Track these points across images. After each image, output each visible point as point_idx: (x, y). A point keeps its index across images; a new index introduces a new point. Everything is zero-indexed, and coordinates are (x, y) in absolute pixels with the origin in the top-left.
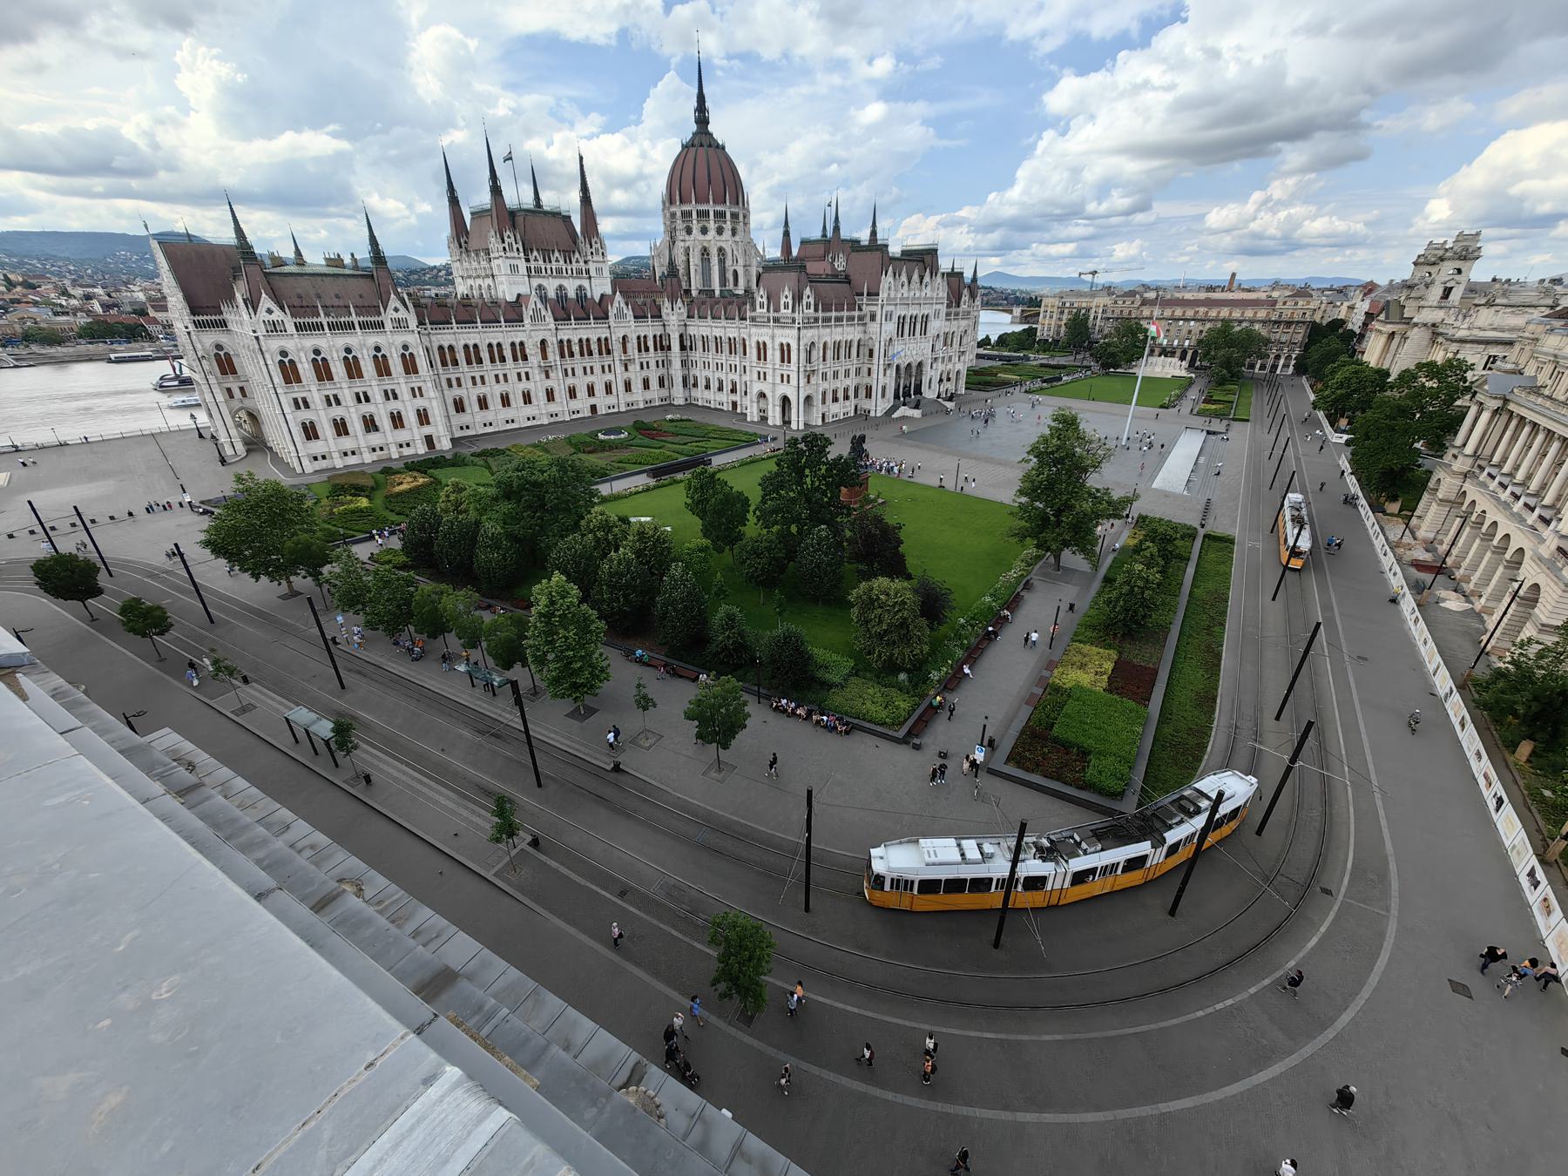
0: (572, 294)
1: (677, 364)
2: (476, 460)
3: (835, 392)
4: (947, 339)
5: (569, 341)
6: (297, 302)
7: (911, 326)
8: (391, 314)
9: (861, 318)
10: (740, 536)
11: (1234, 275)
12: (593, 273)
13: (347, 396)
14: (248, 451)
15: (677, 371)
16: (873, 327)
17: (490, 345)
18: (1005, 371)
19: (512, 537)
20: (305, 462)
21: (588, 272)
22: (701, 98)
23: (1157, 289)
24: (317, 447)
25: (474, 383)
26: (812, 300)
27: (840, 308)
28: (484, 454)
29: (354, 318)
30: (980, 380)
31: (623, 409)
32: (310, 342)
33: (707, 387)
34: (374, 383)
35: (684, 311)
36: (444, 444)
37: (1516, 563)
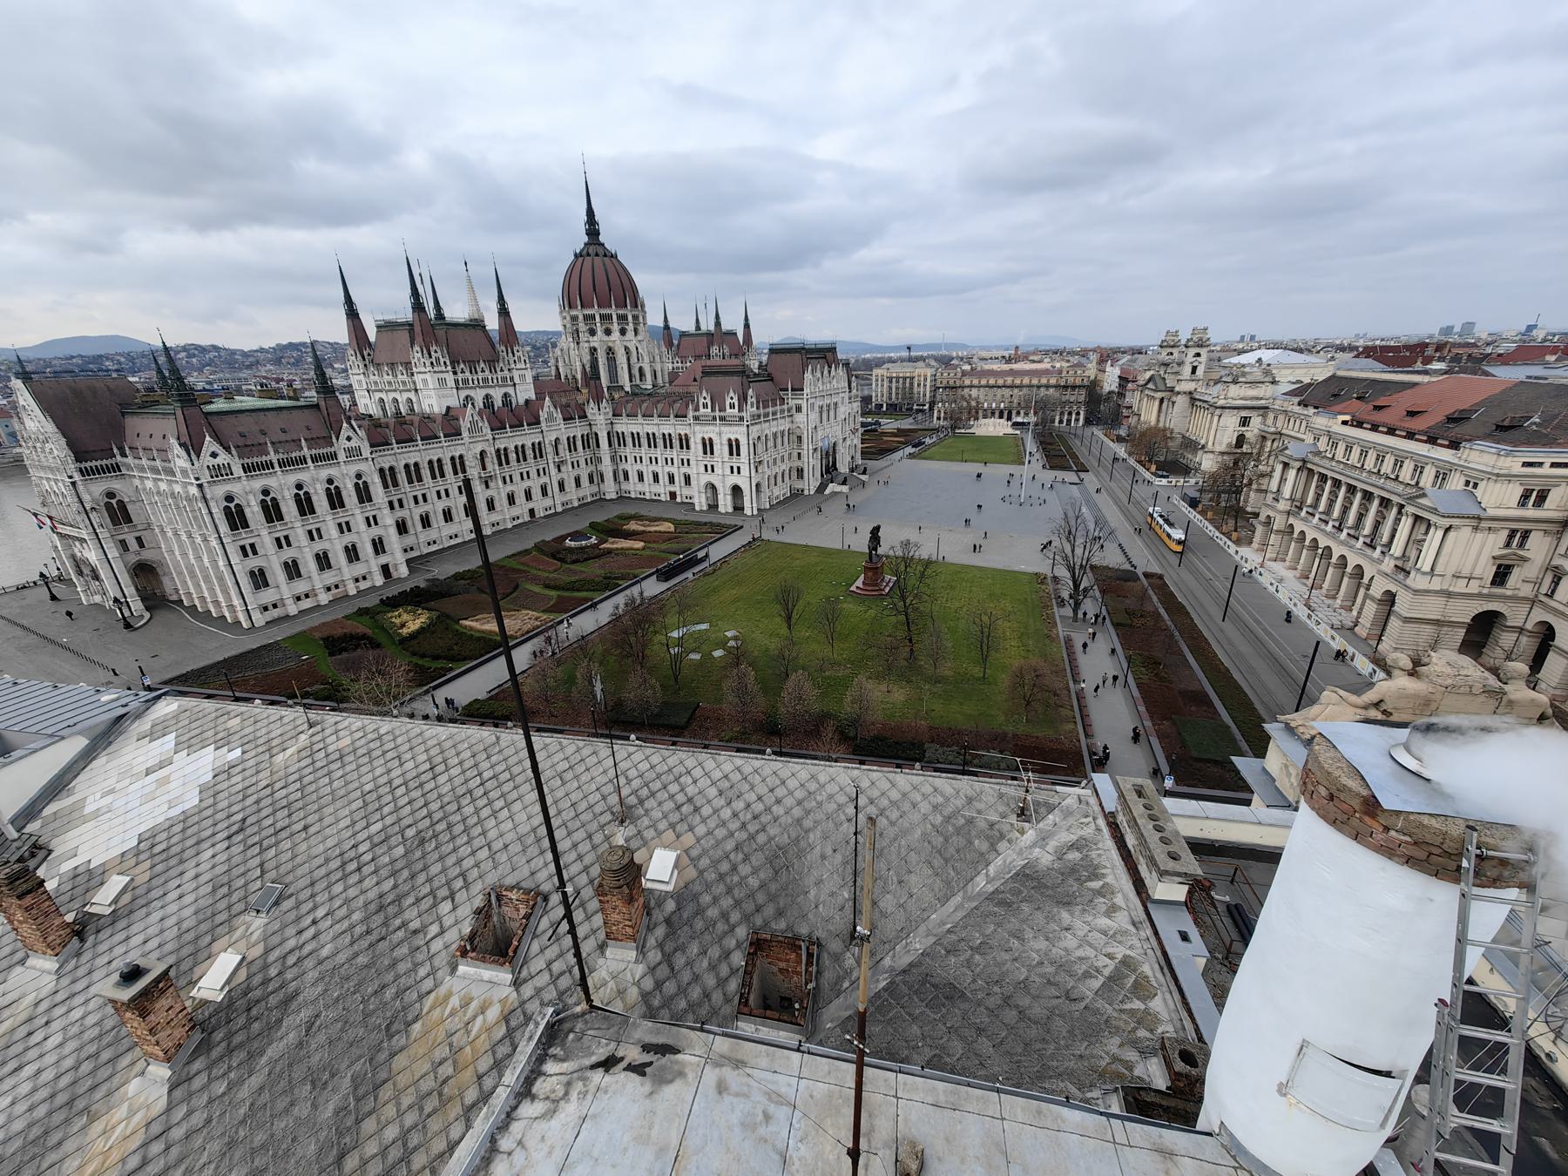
0: (498, 403)
1: (606, 460)
7: (827, 411)
12: (517, 380)
15: (607, 467)
16: (800, 418)
17: (430, 462)
21: (512, 379)
22: (590, 213)
24: (268, 596)
25: (416, 502)
28: (458, 577)
29: (306, 452)
31: (559, 509)
35: (609, 410)
36: (403, 571)
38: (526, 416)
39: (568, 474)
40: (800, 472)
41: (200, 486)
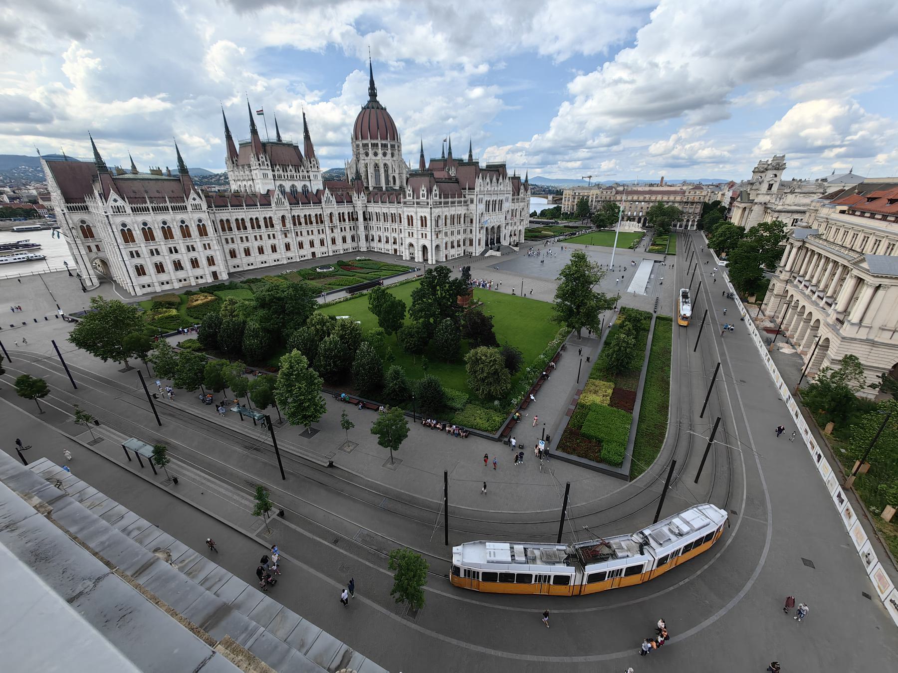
0: (300, 190)
2: (243, 285)
3: (452, 243)
4: (513, 213)
5: (298, 216)
6: (132, 195)
7: (493, 206)
8: (191, 201)
9: (465, 202)
10: (401, 326)
12: (312, 178)
13: (164, 249)
14: (101, 283)
16: (472, 207)
17: (251, 219)
18: (545, 230)
19: (265, 330)
20: (137, 289)
21: (309, 177)
22: (372, 82)
23: (623, 186)
24: (144, 280)
25: (242, 241)
27: (453, 197)
28: (249, 281)
29: (168, 204)
30: (532, 235)
31: (331, 254)
32: (141, 218)
33: (380, 241)
34: (181, 242)
35: (365, 199)
36: (224, 276)
37: (816, 327)
38: (315, 199)
39: (338, 235)
41: (107, 216)
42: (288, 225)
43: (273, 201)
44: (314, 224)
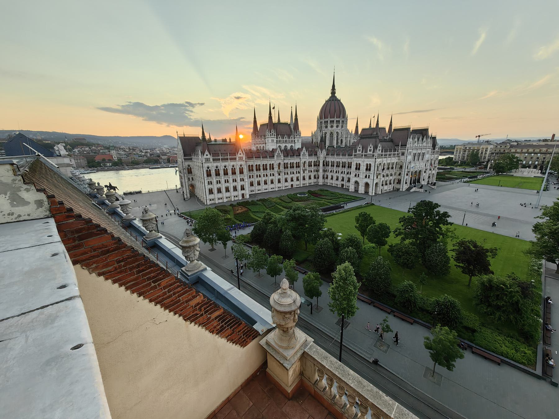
0: (289, 148)
2: (258, 202)
7: (418, 157)
11: (554, 135)
13: (223, 181)
15: (321, 173)
19: (294, 236)
20: (208, 201)
23: (516, 141)
24: (212, 196)
26: (381, 148)
28: (260, 200)
30: (441, 177)
31: (302, 186)
33: (332, 178)
35: (325, 153)
36: (248, 197)
38: (295, 153)
39: (307, 174)
40: (399, 182)
42: (281, 168)
43: (276, 154)
44: (295, 168)
